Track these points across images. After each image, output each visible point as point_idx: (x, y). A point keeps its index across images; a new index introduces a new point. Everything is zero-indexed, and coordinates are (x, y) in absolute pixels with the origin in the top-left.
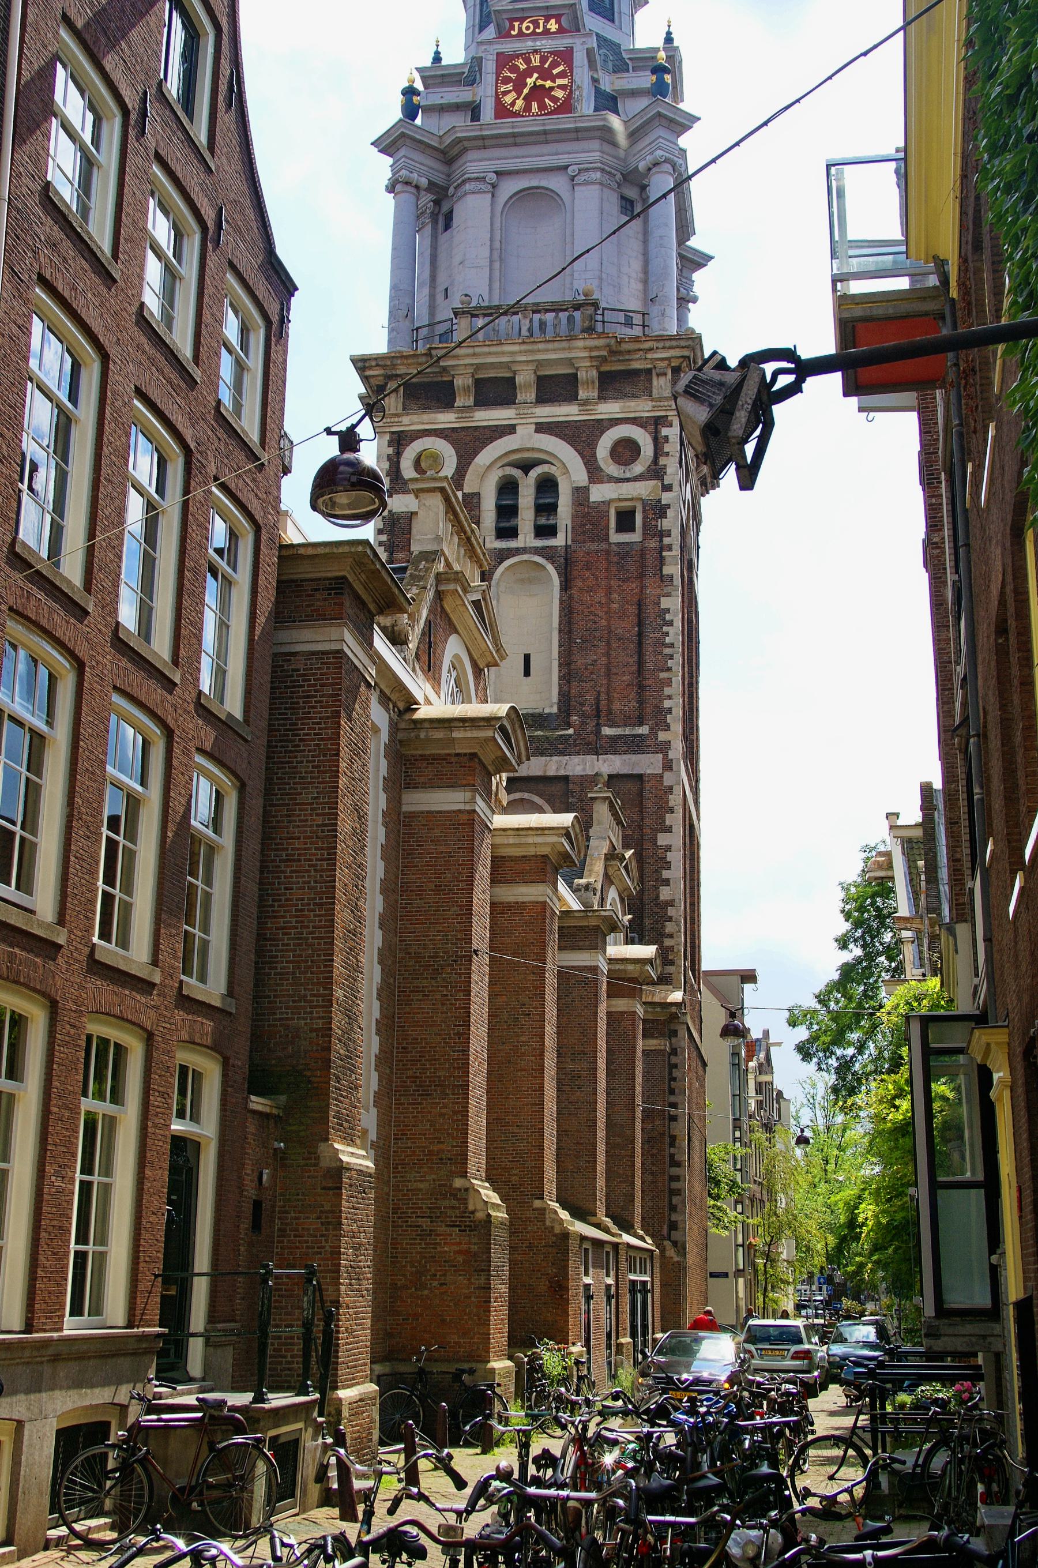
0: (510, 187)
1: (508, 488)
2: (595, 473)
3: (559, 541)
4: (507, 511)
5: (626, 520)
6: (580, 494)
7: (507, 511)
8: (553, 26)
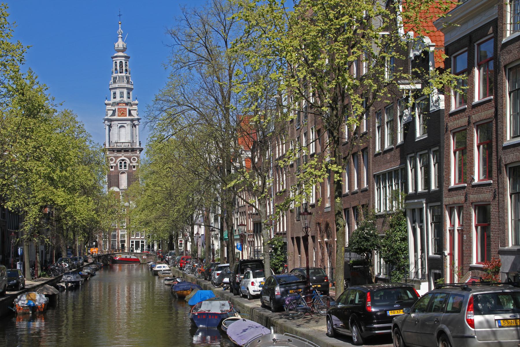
0: (119, 125)
1: (121, 163)
2: (131, 162)
3: (127, 169)
4: (121, 166)
5: (134, 167)
6: (129, 164)
7: (121, 166)
8: (124, 105)
